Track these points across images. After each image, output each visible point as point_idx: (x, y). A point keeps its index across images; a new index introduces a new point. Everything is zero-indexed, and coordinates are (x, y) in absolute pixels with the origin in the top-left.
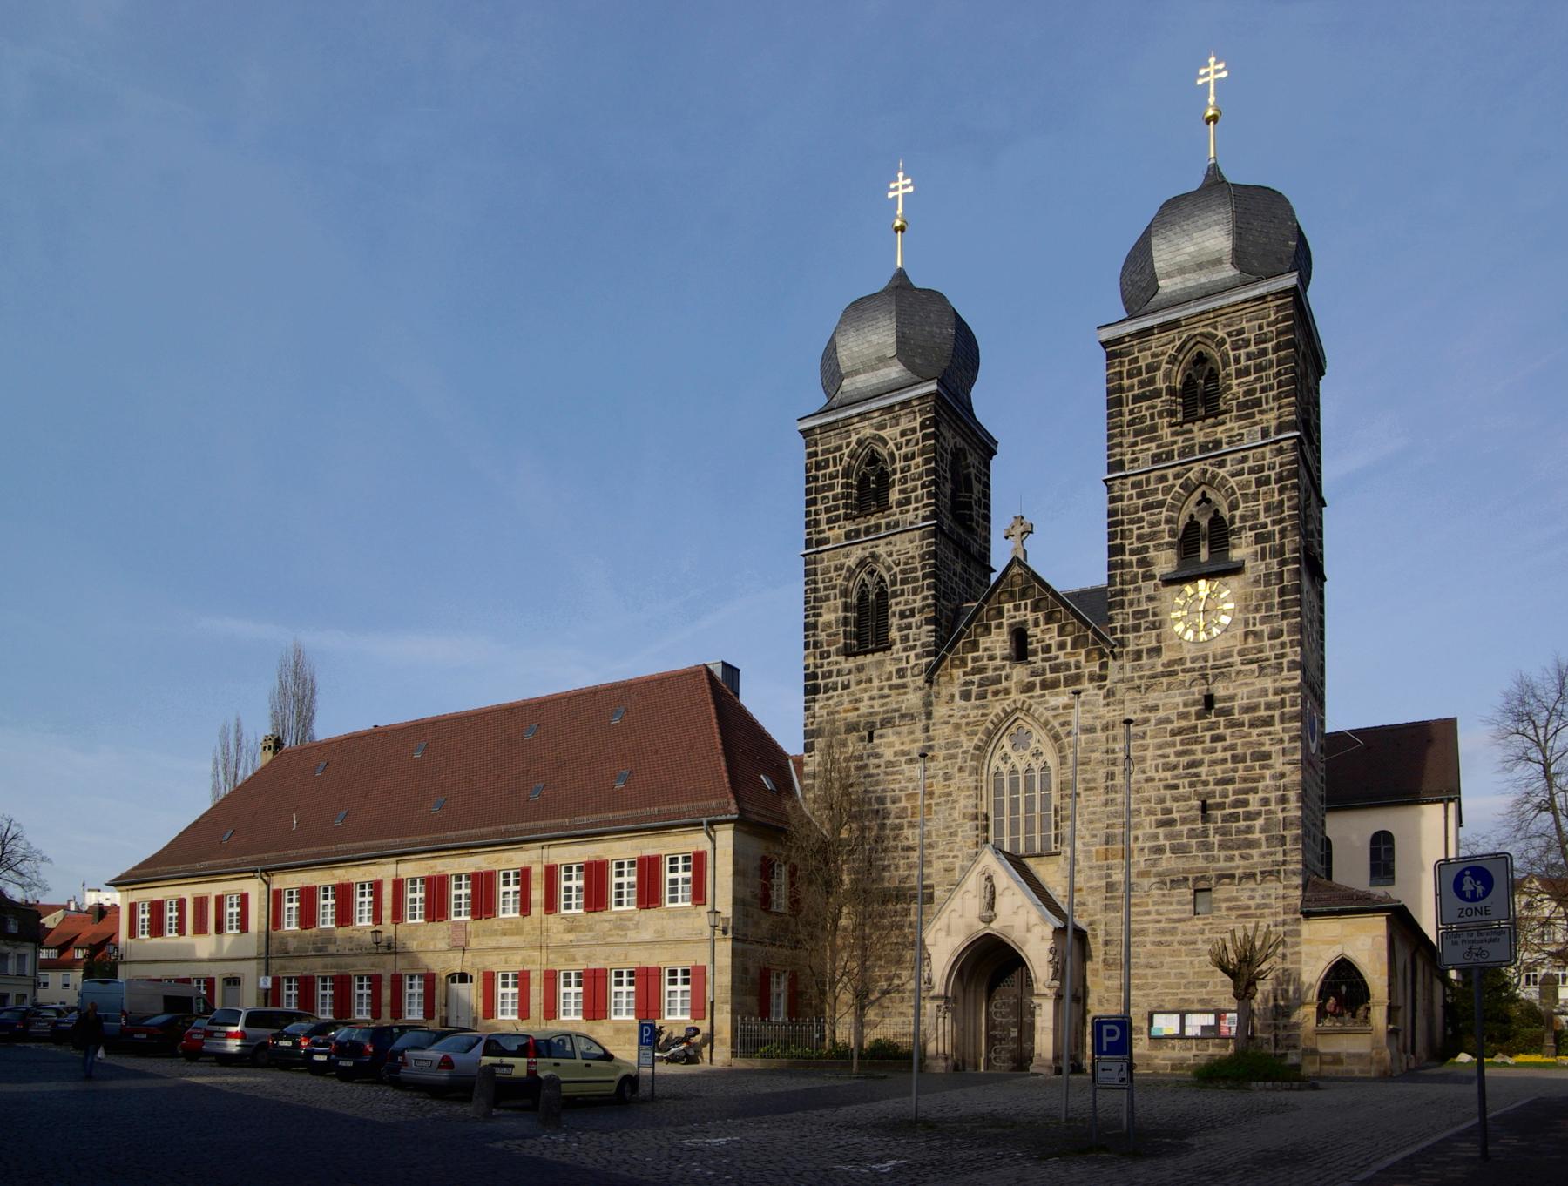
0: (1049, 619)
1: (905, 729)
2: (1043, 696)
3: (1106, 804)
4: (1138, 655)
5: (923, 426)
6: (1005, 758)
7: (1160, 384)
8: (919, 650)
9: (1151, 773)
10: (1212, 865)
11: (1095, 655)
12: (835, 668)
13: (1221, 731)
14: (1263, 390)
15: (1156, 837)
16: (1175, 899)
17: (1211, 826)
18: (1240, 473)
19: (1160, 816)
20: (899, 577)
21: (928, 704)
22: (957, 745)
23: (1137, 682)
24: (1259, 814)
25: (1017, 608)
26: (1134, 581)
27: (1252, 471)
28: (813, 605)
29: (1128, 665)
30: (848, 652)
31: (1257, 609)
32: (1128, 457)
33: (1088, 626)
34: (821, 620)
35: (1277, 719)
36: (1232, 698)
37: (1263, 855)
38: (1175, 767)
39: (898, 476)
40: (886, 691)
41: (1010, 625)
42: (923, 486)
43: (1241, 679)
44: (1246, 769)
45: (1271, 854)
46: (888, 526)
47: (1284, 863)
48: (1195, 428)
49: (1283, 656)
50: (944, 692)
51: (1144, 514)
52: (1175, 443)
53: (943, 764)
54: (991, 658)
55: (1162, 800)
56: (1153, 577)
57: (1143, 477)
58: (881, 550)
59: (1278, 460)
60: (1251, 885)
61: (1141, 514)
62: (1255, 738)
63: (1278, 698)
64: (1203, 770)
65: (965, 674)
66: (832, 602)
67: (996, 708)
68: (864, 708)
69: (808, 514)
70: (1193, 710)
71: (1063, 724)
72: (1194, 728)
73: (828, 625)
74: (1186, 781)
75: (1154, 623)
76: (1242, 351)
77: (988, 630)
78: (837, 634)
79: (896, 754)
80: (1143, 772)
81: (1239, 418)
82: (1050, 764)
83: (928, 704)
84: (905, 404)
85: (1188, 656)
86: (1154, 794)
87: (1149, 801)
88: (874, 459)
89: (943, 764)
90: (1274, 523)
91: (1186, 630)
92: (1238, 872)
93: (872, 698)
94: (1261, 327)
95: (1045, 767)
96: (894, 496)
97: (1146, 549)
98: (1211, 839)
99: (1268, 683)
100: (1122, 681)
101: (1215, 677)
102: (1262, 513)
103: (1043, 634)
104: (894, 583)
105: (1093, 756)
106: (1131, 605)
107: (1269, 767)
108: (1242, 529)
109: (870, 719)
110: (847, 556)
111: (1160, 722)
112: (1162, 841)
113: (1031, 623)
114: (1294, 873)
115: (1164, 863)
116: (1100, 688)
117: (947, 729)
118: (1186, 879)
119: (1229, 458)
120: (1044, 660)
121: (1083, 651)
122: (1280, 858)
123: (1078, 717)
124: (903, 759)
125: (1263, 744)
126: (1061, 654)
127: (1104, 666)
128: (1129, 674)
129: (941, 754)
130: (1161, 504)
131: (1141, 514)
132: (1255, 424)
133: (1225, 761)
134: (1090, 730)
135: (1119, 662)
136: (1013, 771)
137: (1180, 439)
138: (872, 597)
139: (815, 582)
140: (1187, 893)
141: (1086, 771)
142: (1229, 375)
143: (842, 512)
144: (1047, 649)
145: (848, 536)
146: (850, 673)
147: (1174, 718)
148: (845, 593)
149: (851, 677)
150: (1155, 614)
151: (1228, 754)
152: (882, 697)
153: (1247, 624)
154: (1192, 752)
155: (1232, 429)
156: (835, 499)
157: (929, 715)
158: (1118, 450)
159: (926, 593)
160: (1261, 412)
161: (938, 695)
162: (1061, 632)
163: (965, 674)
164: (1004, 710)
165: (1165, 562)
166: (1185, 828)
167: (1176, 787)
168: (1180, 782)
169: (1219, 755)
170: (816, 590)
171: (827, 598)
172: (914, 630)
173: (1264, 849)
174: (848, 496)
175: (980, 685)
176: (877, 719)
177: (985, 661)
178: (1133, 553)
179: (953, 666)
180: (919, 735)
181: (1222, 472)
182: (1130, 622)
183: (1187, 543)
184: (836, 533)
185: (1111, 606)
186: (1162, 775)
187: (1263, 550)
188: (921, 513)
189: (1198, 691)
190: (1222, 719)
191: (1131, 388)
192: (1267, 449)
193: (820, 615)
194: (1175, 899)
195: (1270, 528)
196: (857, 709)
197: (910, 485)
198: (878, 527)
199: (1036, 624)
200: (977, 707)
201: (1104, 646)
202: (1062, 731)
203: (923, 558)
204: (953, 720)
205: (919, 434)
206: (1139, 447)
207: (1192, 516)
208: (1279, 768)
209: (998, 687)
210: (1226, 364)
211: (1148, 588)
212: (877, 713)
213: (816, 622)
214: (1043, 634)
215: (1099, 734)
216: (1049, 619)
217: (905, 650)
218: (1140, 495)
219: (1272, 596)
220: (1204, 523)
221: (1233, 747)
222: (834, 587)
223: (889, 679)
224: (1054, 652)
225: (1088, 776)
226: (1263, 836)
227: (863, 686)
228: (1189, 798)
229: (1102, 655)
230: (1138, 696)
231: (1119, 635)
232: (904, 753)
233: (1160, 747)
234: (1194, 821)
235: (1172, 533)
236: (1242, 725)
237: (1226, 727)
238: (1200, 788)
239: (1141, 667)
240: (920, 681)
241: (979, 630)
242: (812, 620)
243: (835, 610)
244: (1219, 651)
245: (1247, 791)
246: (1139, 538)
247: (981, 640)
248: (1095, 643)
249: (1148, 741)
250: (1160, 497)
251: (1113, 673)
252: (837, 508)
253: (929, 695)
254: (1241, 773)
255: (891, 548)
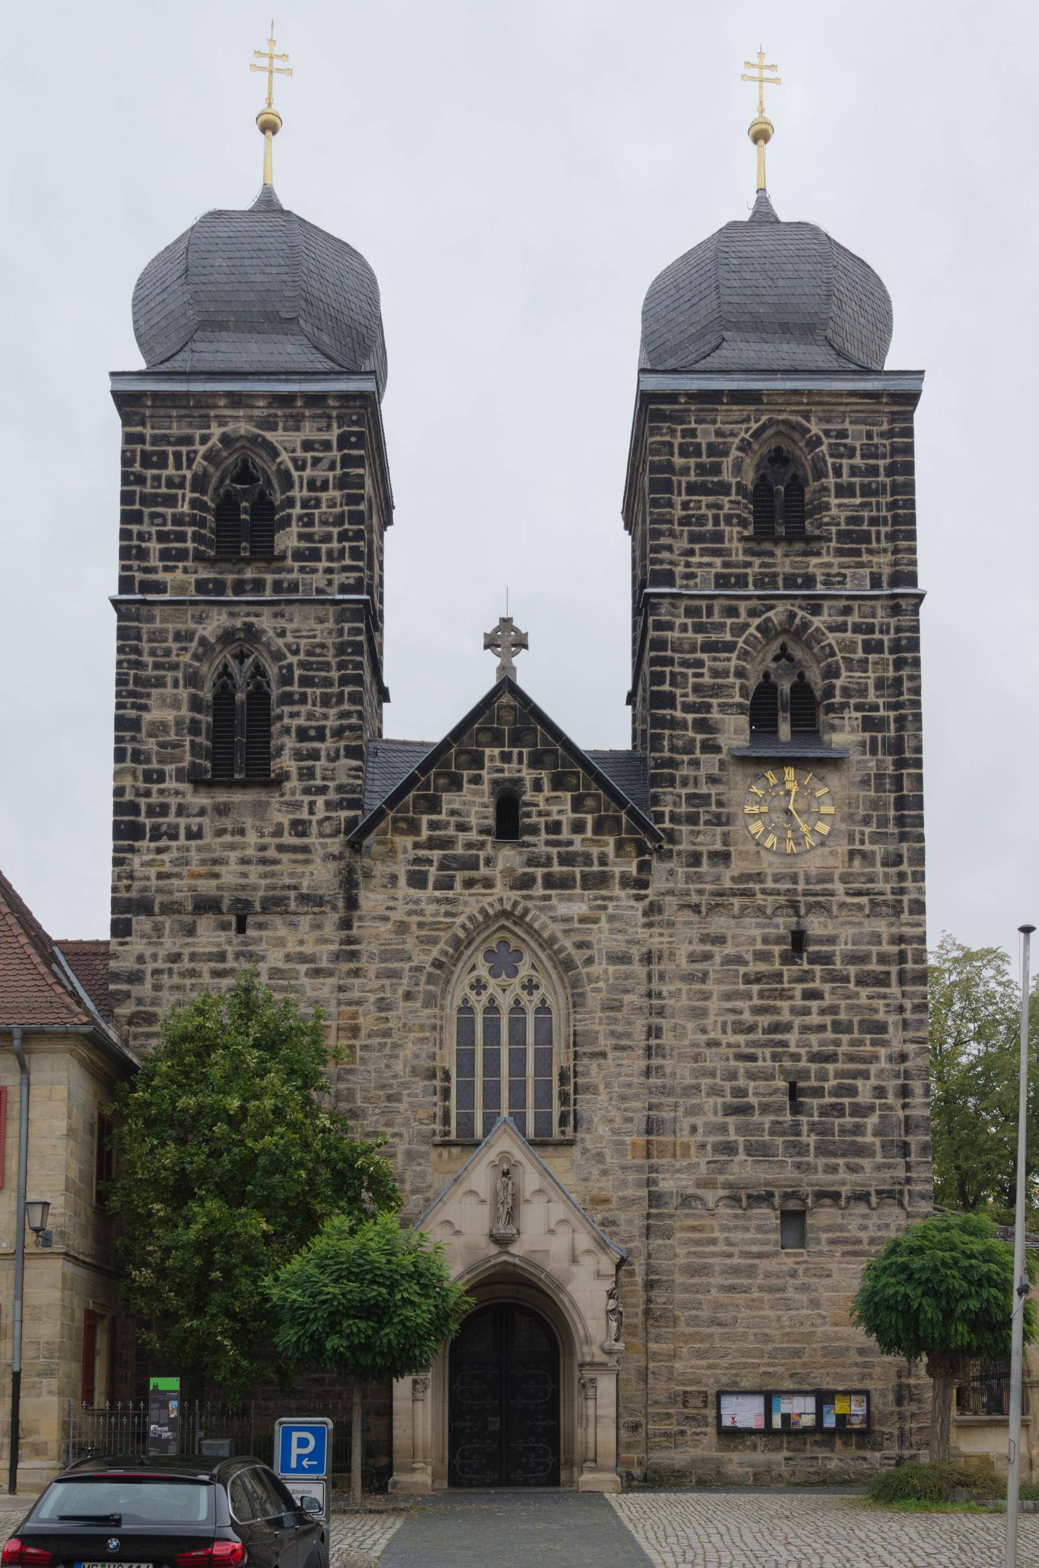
0: (558, 783)
1: (305, 921)
2: (548, 898)
3: (648, 1072)
4: (695, 859)
5: (343, 441)
6: (478, 986)
7: (727, 476)
8: (332, 796)
9: (715, 1035)
10: (807, 1178)
11: (630, 849)
12: (173, 802)
13: (817, 984)
14: (874, 521)
15: (723, 1129)
16: (754, 1222)
17: (803, 1119)
18: (842, 628)
19: (729, 1099)
20: (297, 673)
21: (349, 884)
22: (403, 956)
23: (695, 899)
24: (871, 1108)
25: (506, 758)
26: (689, 749)
27: (857, 629)
28: (133, 685)
29: (681, 871)
30: (196, 779)
31: (866, 821)
32: (680, 570)
33: (621, 803)
34: (147, 717)
35: (894, 978)
36: (832, 940)
37: (878, 1168)
38: (751, 1029)
39: (297, 511)
40: (272, 853)
41: (495, 782)
42: (343, 537)
43: (844, 916)
44: (853, 1043)
45: (889, 1166)
46: (278, 587)
47: (908, 1181)
48: (779, 551)
49: (902, 891)
50: (380, 869)
51: (704, 656)
52: (748, 565)
53: (375, 984)
54: (462, 827)
55: (732, 1076)
56: (717, 749)
57: (703, 603)
58: (265, 622)
59: (893, 621)
60: (862, 1209)
61: (699, 655)
62: (863, 1001)
63: (894, 949)
64: (792, 1037)
65: (416, 846)
66: (169, 690)
67: (472, 904)
68: (229, 874)
69: (125, 535)
70: (777, 949)
71: (580, 945)
72: (778, 976)
73: (160, 727)
74: (768, 1051)
75: (718, 816)
76: (845, 462)
77: (455, 784)
78: (177, 745)
79: (288, 958)
80: (704, 1031)
81: (840, 552)
82: (550, 1002)
83: (349, 884)
84: (315, 400)
85: (769, 871)
86: (719, 1065)
87: (712, 1074)
88: (245, 474)
89: (375, 984)
90: (889, 706)
91: (766, 833)
92: (845, 1190)
93: (244, 861)
94: (869, 435)
95: (543, 1009)
96: (288, 540)
97: (708, 707)
98: (804, 1138)
99: (882, 927)
100: (671, 892)
101: (811, 907)
102: (871, 690)
103: (548, 804)
104: (286, 679)
105: (627, 998)
106: (685, 783)
107: (885, 1043)
108: (844, 706)
109: (243, 895)
110: (200, 619)
111: (728, 960)
112: (732, 1137)
113: (528, 784)
114: (923, 1196)
115: (736, 1169)
116: (639, 898)
117: (384, 928)
118: (770, 1195)
119: (826, 604)
120: (548, 843)
121: (611, 840)
122: (901, 1174)
123: (603, 937)
124: (303, 968)
125: (876, 1011)
126: (577, 838)
127: (644, 866)
128: (681, 885)
129: (372, 968)
130: (730, 647)
131: (699, 655)
132: (861, 565)
133: (822, 1028)
134: (623, 959)
135: (668, 865)
136: (492, 1008)
137: (757, 561)
138: (240, 696)
139: (137, 651)
140: (770, 1217)
141: (616, 1021)
142: (826, 489)
143: (190, 545)
144: (555, 827)
145: (201, 586)
146: (202, 812)
147: (749, 957)
148: (193, 680)
149: (205, 821)
150: (720, 804)
151: (828, 1020)
152: (264, 861)
153: (851, 839)
154: (776, 1011)
155: (830, 565)
156: (178, 520)
157: (352, 904)
158: (665, 555)
159: (347, 706)
160: (870, 552)
161: (368, 875)
162: (577, 805)
163: (416, 846)
164: (483, 911)
165: (734, 731)
166: (767, 1120)
167: (752, 1058)
168: (759, 1051)
169: (815, 1019)
170: (139, 665)
171: (160, 683)
172: (323, 762)
173: (879, 1159)
174: (202, 523)
175: (442, 867)
176: (257, 898)
177: (451, 831)
178: (687, 708)
179: (397, 831)
180: (330, 930)
181: (817, 621)
182: (684, 809)
183: (762, 709)
184: (180, 578)
185: (656, 781)
186: (733, 1038)
187: (874, 740)
188: (338, 578)
189: (783, 924)
190: (817, 968)
191: (685, 471)
192: (878, 604)
193: (145, 708)
194: (754, 1222)
195: (882, 713)
196: (216, 876)
197: (317, 529)
198: (258, 586)
199: (537, 787)
200: (438, 901)
201: (647, 839)
202: (579, 956)
203: (341, 649)
204: (397, 916)
205: (336, 454)
206: (694, 560)
207: (766, 675)
208: (897, 1047)
209: (474, 874)
210: (820, 474)
211: (710, 763)
212: (255, 888)
213: (139, 719)
214: (548, 804)
215: (639, 970)
216: (558, 783)
217: (307, 791)
218: (699, 628)
219: (885, 806)
220: (785, 686)
221: (833, 1010)
222: (174, 667)
223: (278, 833)
224: (565, 834)
225: (619, 1028)
226: (877, 1141)
227: (228, 838)
228: (772, 1077)
229: (641, 850)
230: (694, 918)
231: (667, 825)
232: (303, 959)
233: (728, 997)
234: (780, 1110)
235: (743, 687)
236: (847, 980)
237: (824, 980)
238: (788, 1064)
239: (700, 878)
240: (335, 845)
241: (442, 781)
242: (131, 713)
243: (176, 705)
244: (814, 872)
245: (855, 1075)
246: (697, 689)
247: (445, 796)
248: (630, 830)
249: (709, 986)
250: (728, 637)
251: (659, 883)
252: (181, 537)
253: (351, 870)
254: (844, 1048)
255: (281, 623)
